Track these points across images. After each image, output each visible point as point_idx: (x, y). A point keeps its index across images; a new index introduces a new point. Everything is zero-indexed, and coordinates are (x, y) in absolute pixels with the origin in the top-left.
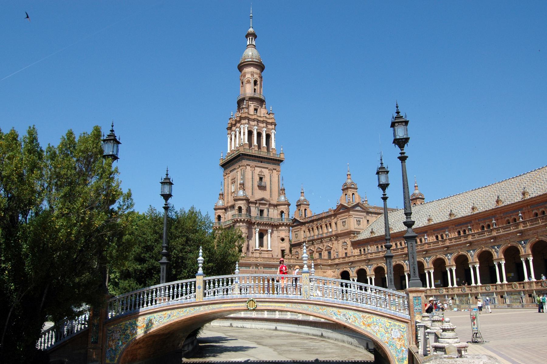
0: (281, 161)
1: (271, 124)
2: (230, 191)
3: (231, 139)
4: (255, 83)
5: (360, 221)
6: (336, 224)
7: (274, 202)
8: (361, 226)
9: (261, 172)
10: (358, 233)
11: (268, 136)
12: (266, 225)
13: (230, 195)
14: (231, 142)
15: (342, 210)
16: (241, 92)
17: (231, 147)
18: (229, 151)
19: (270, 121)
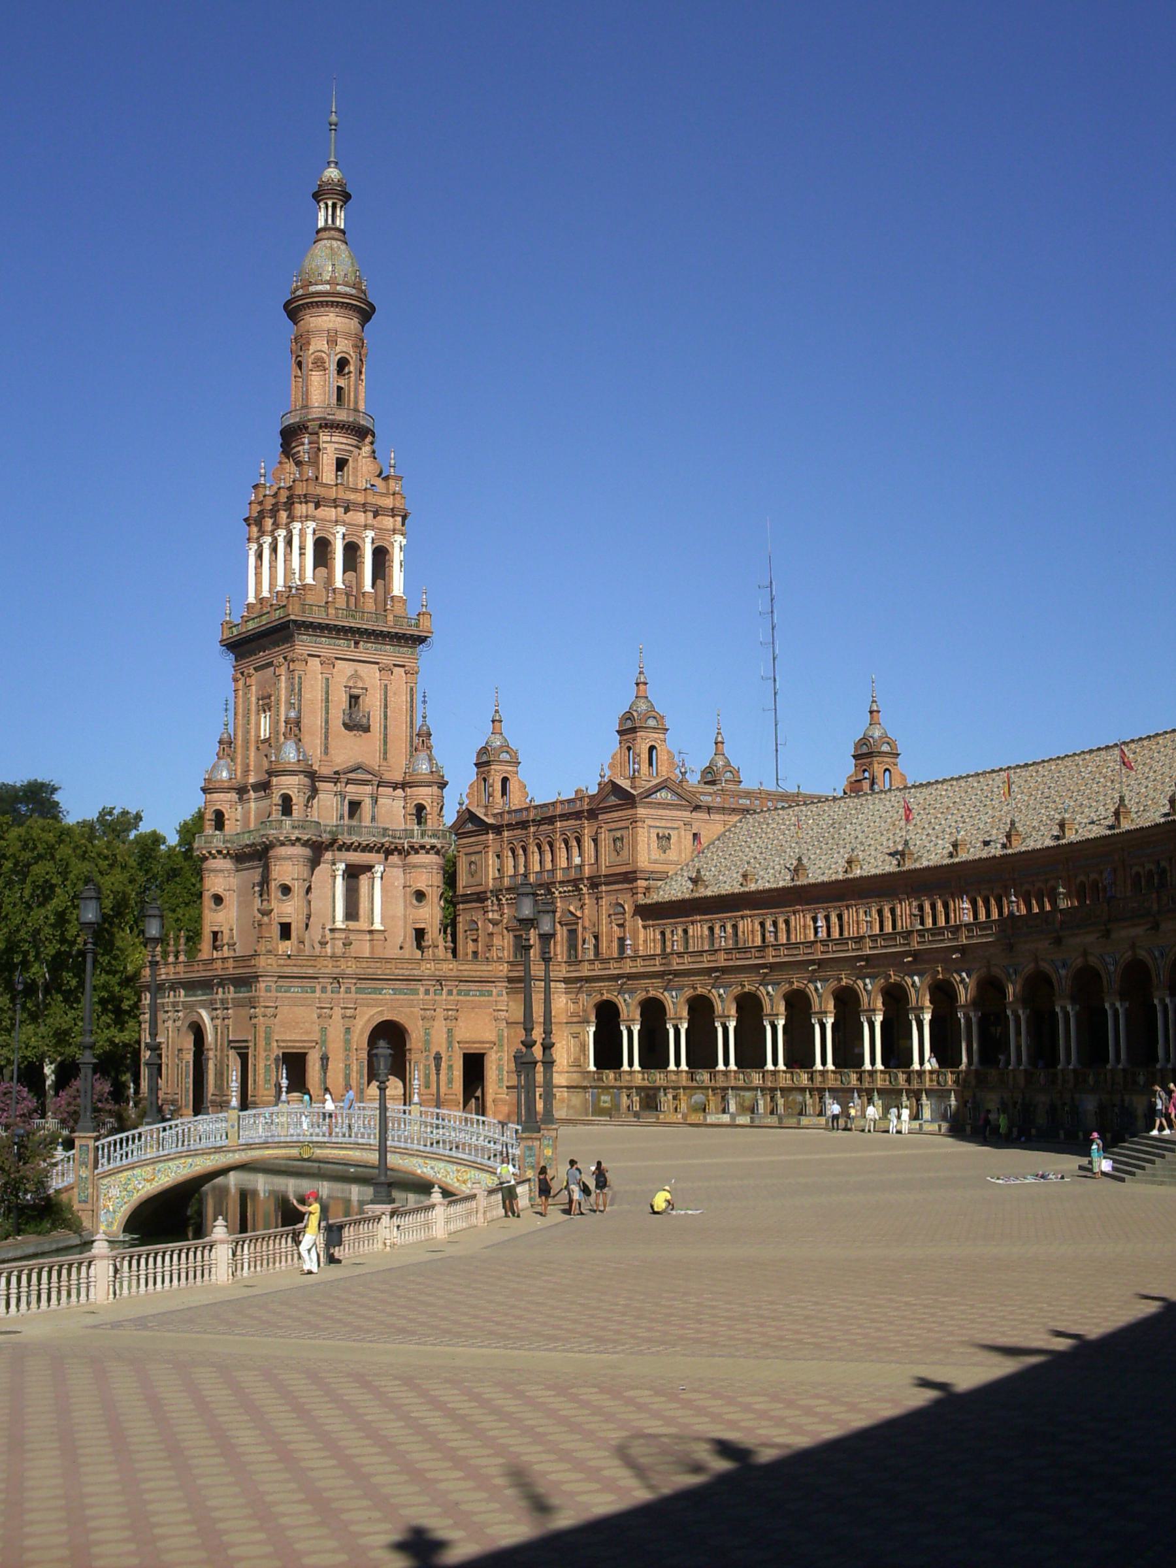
0: (421, 640)
1: (393, 512)
2: (253, 733)
3: (259, 556)
4: (342, 364)
5: (669, 838)
6: (595, 841)
7: (398, 777)
8: (672, 855)
9: (356, 676)
10: (664, 877)
11: (381, 555)
12: (367, 849)
13: (253, 749)
14: (259, 567)
15: (616, 799)
16: (295, 396)
17: (258, 583)
18: (251, 599)
19: (388, 502)
